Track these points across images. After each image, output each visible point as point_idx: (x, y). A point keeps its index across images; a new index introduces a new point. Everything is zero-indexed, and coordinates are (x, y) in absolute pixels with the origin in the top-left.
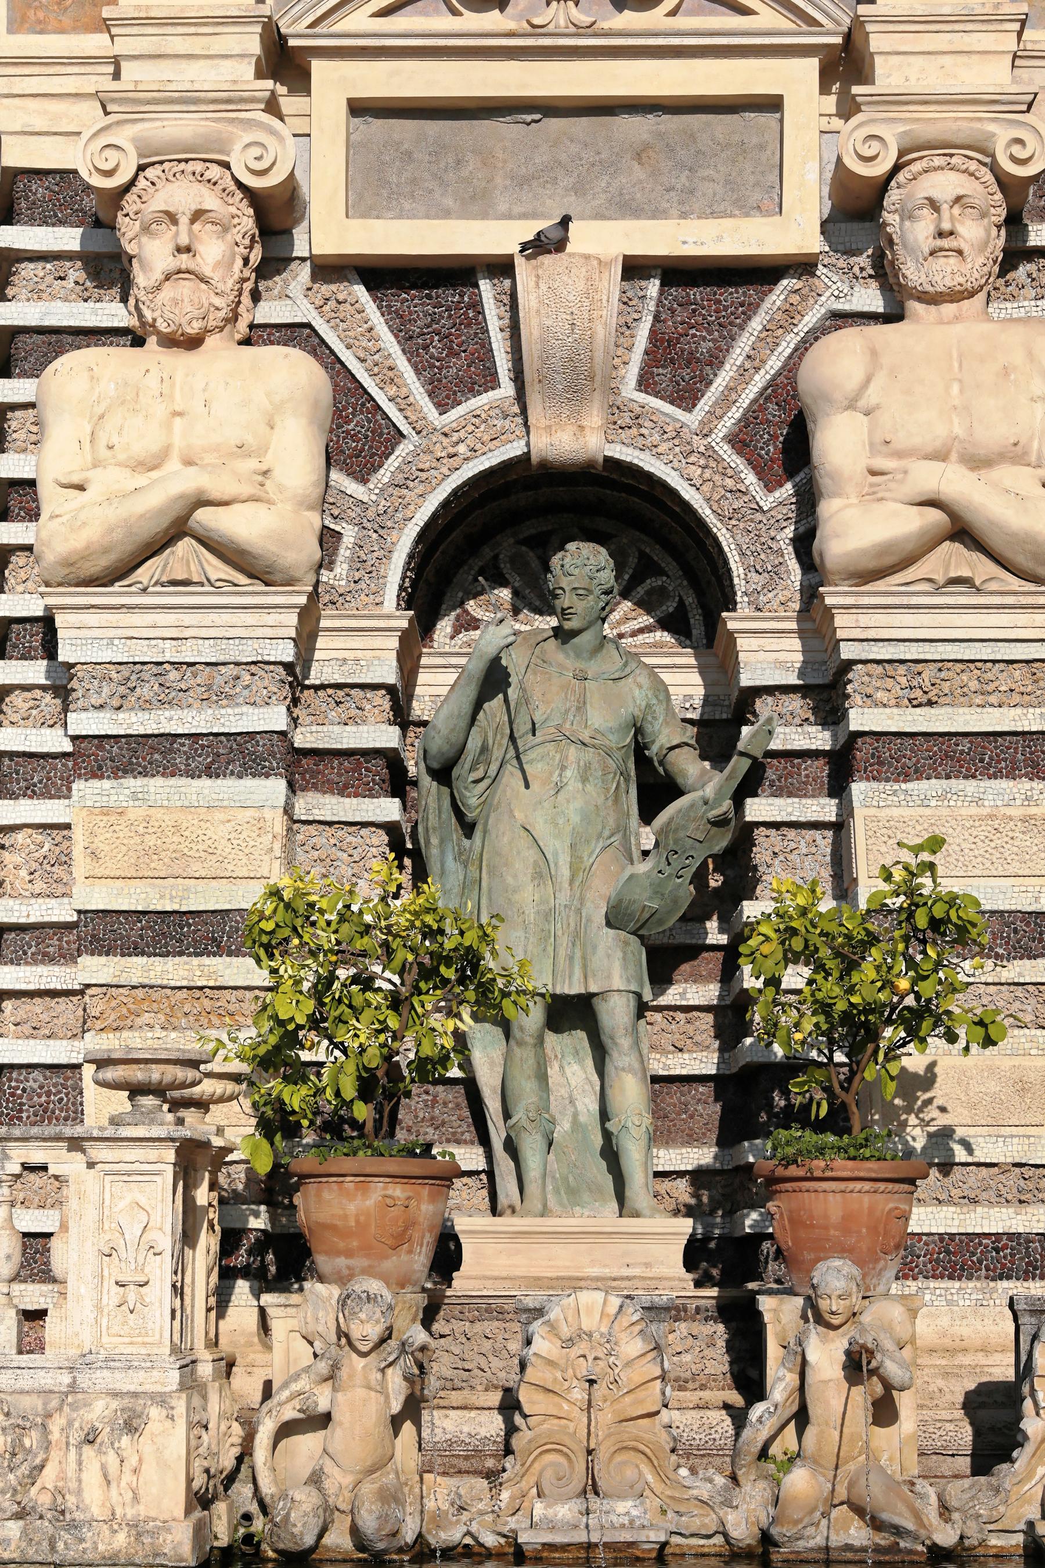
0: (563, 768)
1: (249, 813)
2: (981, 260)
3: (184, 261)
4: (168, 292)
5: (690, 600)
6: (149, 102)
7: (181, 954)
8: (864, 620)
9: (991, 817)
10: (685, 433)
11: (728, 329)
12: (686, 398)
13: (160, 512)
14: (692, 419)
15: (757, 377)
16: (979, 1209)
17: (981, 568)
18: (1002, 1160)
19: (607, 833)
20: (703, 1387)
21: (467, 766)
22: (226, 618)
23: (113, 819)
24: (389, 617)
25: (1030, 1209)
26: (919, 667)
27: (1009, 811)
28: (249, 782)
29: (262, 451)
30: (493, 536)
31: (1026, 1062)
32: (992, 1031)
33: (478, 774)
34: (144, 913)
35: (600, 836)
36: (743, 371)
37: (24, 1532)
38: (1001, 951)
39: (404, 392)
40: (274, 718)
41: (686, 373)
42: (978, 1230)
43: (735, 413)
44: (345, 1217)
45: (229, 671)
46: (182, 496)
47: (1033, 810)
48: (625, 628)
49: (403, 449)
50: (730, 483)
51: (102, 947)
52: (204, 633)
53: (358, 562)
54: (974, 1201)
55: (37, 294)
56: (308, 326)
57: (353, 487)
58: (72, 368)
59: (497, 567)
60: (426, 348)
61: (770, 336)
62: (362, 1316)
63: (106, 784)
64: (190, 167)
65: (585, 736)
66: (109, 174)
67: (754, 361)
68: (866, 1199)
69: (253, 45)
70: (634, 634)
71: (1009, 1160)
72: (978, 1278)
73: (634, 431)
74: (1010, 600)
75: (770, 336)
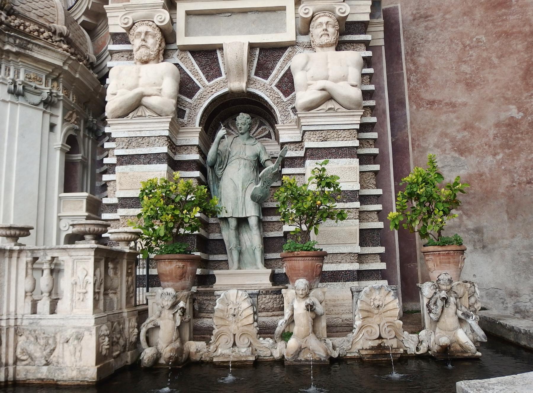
0: (240, 165)
1: (159, 172)
2: (334, 37)
3: (144, 43)
5: (271, 130)
6: (135, 7)
8: (308, 120)
10: (266, 85)
11: (276, 61)
12: (266, 77)
13: (133, 98)
17: (337, 106)
20: (273, 311)
22: (152, 125)
23: (125, 175)
24: (196, 128)
25: (354, 264)
26: (322, 132)
27: (345, 166)
28: (158, 165)
29: (160, 85)
31: (352, 228)
32: (344, 215)
33: (221, 167)
37: (48, 370)
39: (200, 78)
40: (165, 149)
41: (266, 72)
43: (277, 80)
44: (166, 271)
45: (153, 138)
46: (138, 94)
47: (351, 166)
49: (200, 91)
52: (147, 129)
54: (340, 263)
57: (188, 100)
60: (206, 68)
62: (166, 299)
63: (124, 167)
64: (145, 22)
65: (245, 157)
67: (282, 67)
74: (344, 114)
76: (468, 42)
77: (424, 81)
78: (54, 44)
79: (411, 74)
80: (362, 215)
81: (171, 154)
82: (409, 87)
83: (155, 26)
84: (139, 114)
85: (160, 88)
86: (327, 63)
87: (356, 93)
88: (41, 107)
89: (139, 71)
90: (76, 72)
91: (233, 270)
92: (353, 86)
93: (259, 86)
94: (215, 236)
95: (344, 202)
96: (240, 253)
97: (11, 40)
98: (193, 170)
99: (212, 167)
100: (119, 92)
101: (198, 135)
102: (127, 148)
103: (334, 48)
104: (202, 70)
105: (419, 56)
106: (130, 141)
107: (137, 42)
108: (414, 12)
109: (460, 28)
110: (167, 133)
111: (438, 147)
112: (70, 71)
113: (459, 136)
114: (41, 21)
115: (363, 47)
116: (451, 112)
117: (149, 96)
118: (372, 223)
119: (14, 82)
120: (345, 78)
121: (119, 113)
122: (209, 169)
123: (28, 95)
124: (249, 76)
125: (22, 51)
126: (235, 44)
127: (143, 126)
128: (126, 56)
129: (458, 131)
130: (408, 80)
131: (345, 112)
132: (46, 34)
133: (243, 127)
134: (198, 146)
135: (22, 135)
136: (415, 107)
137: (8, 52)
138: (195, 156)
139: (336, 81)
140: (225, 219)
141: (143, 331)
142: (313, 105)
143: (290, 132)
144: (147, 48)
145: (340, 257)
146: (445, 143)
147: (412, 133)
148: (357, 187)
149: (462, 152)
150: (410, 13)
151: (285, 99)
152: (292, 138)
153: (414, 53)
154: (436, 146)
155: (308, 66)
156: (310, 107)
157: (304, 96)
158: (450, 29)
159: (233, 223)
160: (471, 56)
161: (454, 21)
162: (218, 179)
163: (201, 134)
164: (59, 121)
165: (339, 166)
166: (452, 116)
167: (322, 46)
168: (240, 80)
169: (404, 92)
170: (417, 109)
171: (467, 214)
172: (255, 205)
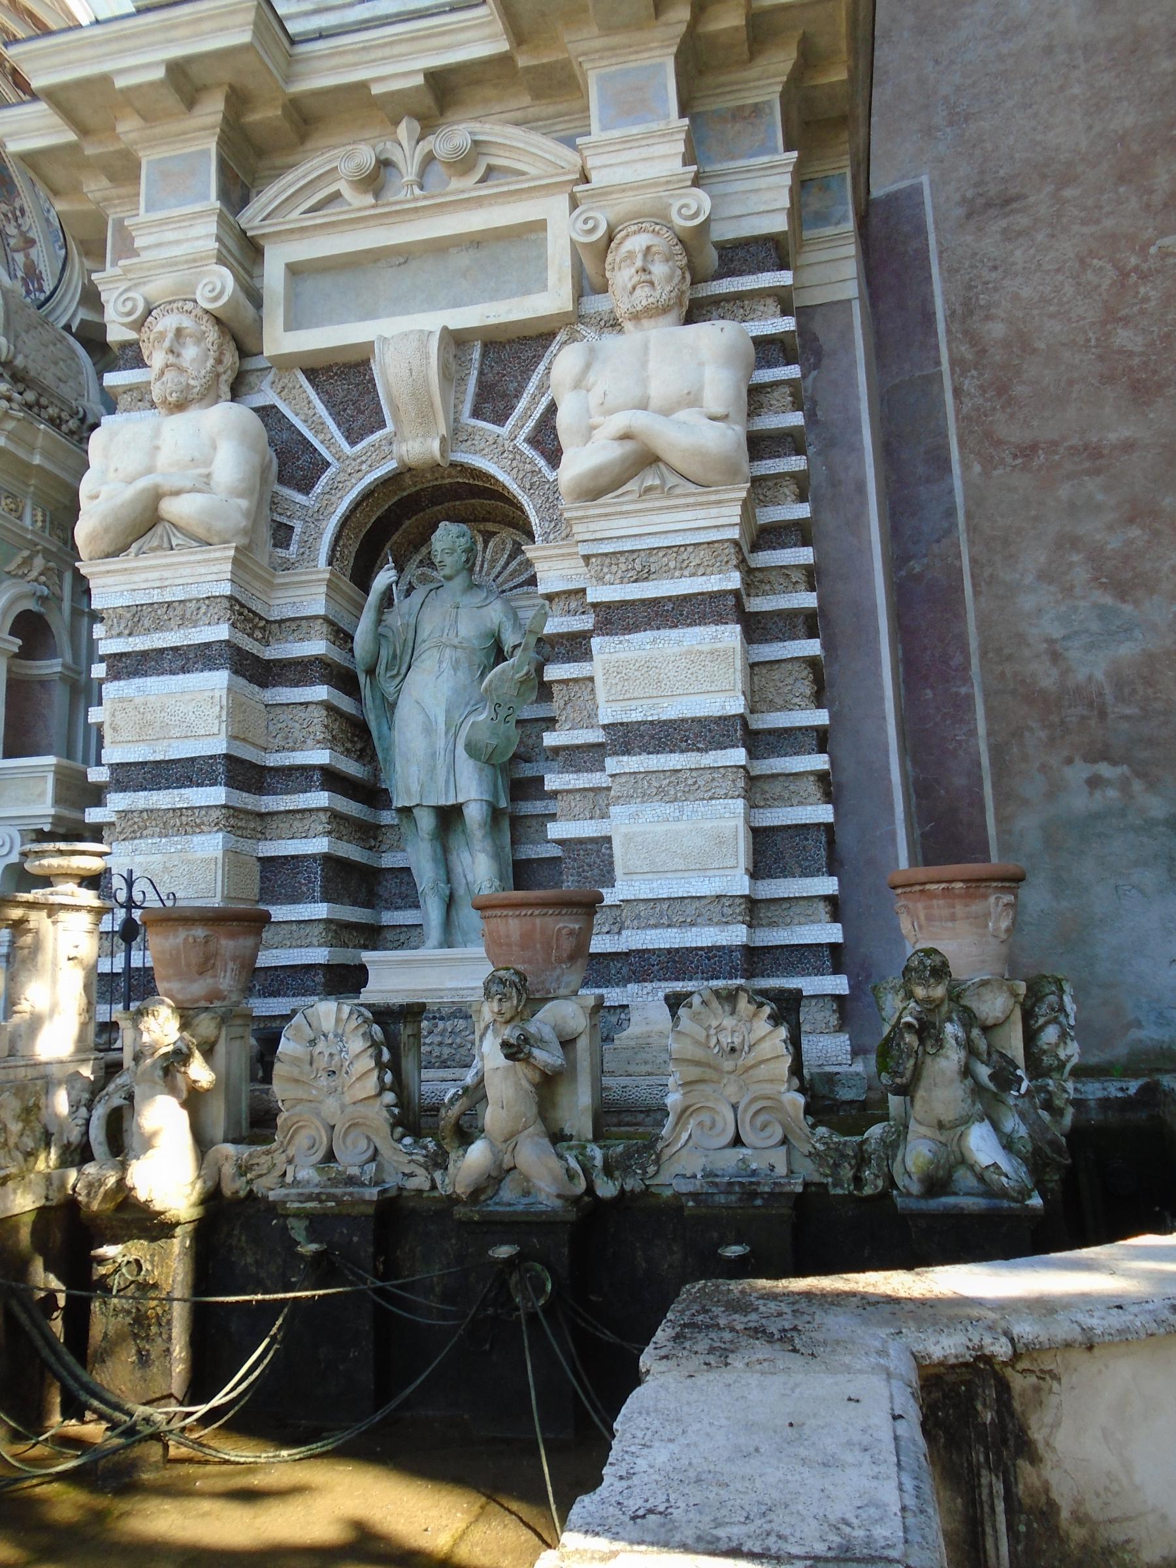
0: (440, 662)
2: (668, 288)
7: (168, 788)
8: (592, 527)
9: (689, 652)
14: (504, 431)
15: (543, 399)
16: (694, 929)
18: (708, 893)
19: (472, 702)
21: (383, 667)
23: (125, 705)
25: (730, 927)
27: (700, 647)
28: (206, 674)
29: (208, 462)
31: (722, 823)
33: (395, 672)
34: (146, 763)
35: (467, 704)
36: (534, 396)
38: (700, 746)
40: (222, 632)
42: (694, 945)
43: (531, 424)
46: (144, 491)
47: (719, 645)
48: (505, 587)
50: (528, 466)
53: (303, 543)
54: (692, 924)
56: (274, 407)
57: (300, 498)
59: (430, 559)
60: (345, 410)
63: (122, 683)
64: (175, 305)
65: (456, 642)
68: (538, 921)
70: (511, 589)
71: (713, 893)
72: (697, 979)
73: (469, 443)
74: (691, 500)
76: (1133, 261)
77: (1002, 390)
79: (964, 373)
80: (754, 787)
81: (250, 645)
82: (958, 411)
83: (199, 312)
86: (644, 364)
87: (722, 438)
89: (157, 433)
90: (32, 449)
91: (428, 952)
92: (713, 418)
93: (483, 445)
94: (389, 860)
95: (698, 750)
98: (313, 684)
99: (371, 672)
100: (105, 491)
102: (130, 635)
103: (673, 316)
104: (335, 416)
105: (988, 318)
106: (137, 617)
107: (157, 359)
108: (969, 194)
109: (1109, 223)
110: (226, 589)
111: (1051, 582)
112: (11, 447)
113: (1114, 543)
115: (772, 306)
116: (1088, 472)
117: (177, 493)
118: (800, 808)
120: (692, 400)
122: (362, 678)
127: (166, 574)
129: (1110, 528)
130: (957, 392)
131: (694, 494)
133: (448, 560)
134: (326, 619)
136: (977, 468)
138: (316, 646)
139: (666, 412)
140: (406, 811)
141: (100, 1111)
142: (603, 481)
143: (567, 563)
144: (181, 370)
145: (691, 909)
146: (1071, 565)
147: (971, 543)
148: (736, 705)
149: (1122, 591)
150: (957, 197)
152: (570, 580)
153: (971, 313)
154: (1044, 576)
155: (591, 378)
156: (599, 488)
157: (580, 461)
158: (1076, 228)
159: (426, 822)
160: (1146, 299)
161: (1090, 203)
162: (389, 707)
163: (330, 584)
165: (684, 649)
166: (1092, 485)
167: (636, 317)
169: (945, 428)
170: (986, 473)
171: (1142, 775)
172: (481, 770)
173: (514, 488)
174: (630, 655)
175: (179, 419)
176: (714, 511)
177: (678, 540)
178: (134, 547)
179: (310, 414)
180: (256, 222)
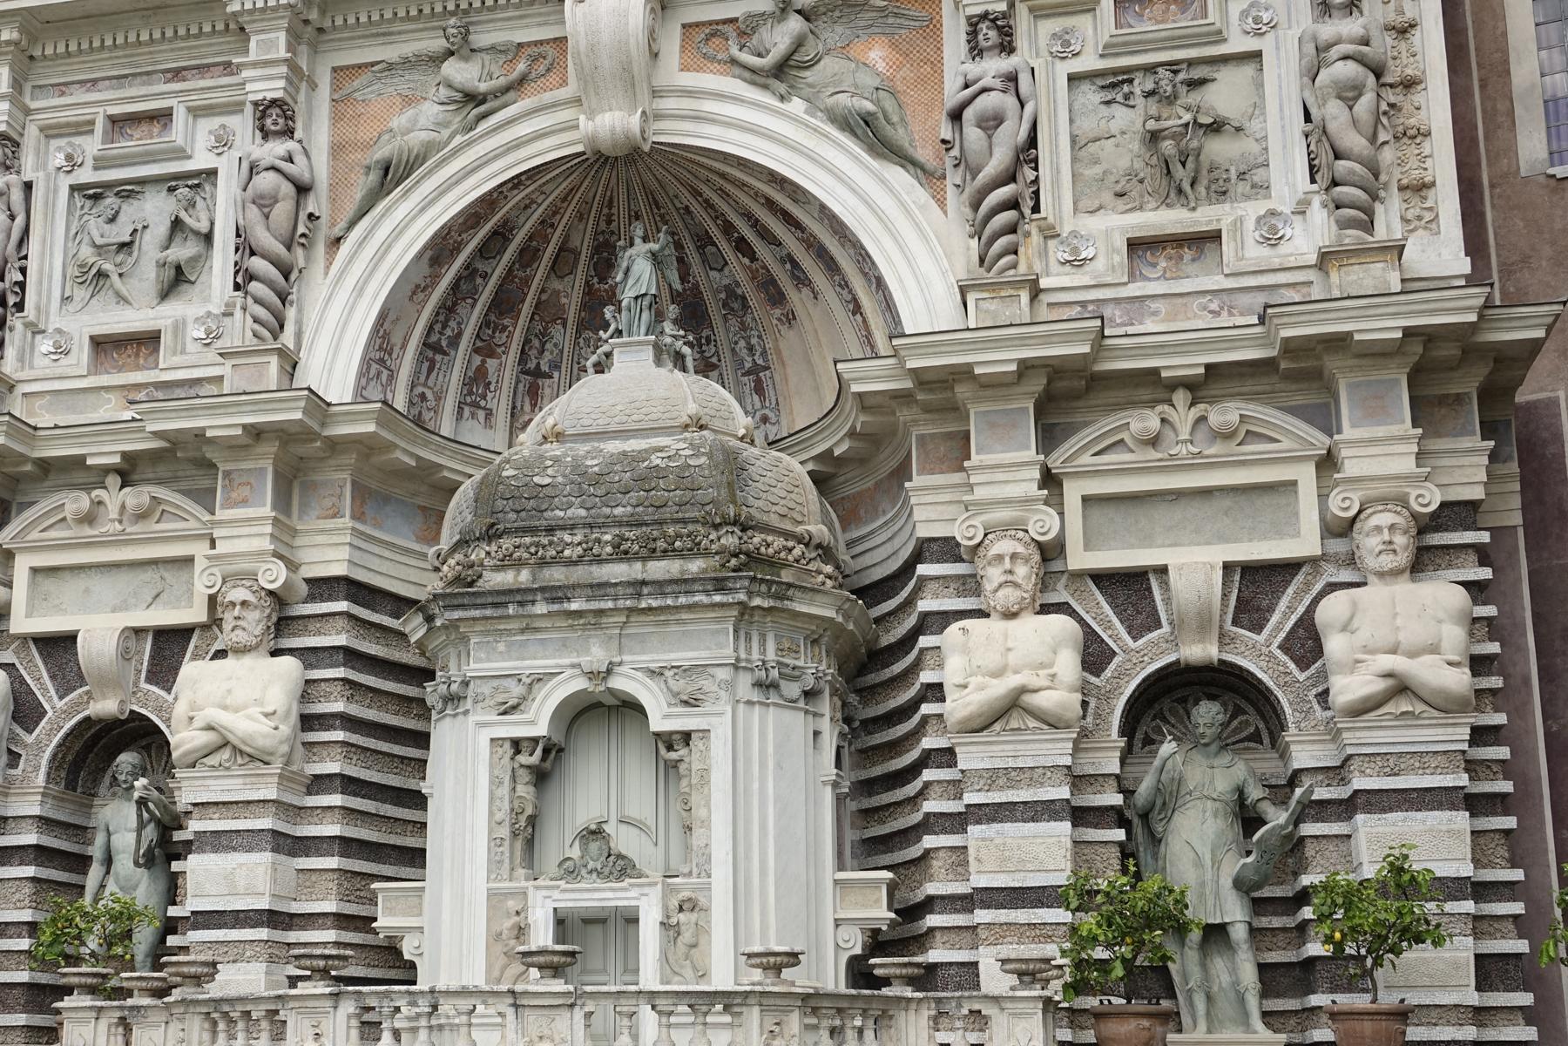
3: (1010, 578)
4: (1000, 593)
12: (1257, 628)
13: (1005, 696)
14: (1261, 638)
22: (1037, 746)
28: (1053, 824)
29: (1051, 665)
30: (1165, 699)
40: (1063, 792)
43: (1283, 635)
45: (1040, 771)
49: (1116, 660)
51: (986, 905)
53: (1097, 715)
55: (936, 596)
58: (954, 628)
61: (1298, 597)
66: (970, 539)
67: (1291, 609)
69: (1037, 475)
75: (1298, 597)
78: (810, 567)
80: (1480, 925)
83: (1027, 539)
84: (1014, 724)
85: (1051, 671)
88: (801, 704)
96: (1209, 998)
97: (764, 588)
100: (974, 681)
101: (1118, 754)
106: (994, 777)
110: (1068, 761)
114: (788, 526)
115: (1473, 557)
119: (764, 662)
121: (976, 724)
123: (783, 683)
124: (1221, 627)
125: (778, 604)
126: (1194, 566)
127: (1019, 747)
128: (953, 585)
132: (797, 552)
135: (779, 766)
137: (758, 607)
143: (1316, 747)
144: (1016, 585)
145: (1434, 1013)
151: (1302, 677)
164: (825, 725)
168: (1201, 641)
173: (1270, 684)
174: (1387, 829)
175: (1012, 624)
176: (1450, 730)
177: (1423, 748)
178: (997, 727)
179: (1101, 611)
180: (1058, 464)
